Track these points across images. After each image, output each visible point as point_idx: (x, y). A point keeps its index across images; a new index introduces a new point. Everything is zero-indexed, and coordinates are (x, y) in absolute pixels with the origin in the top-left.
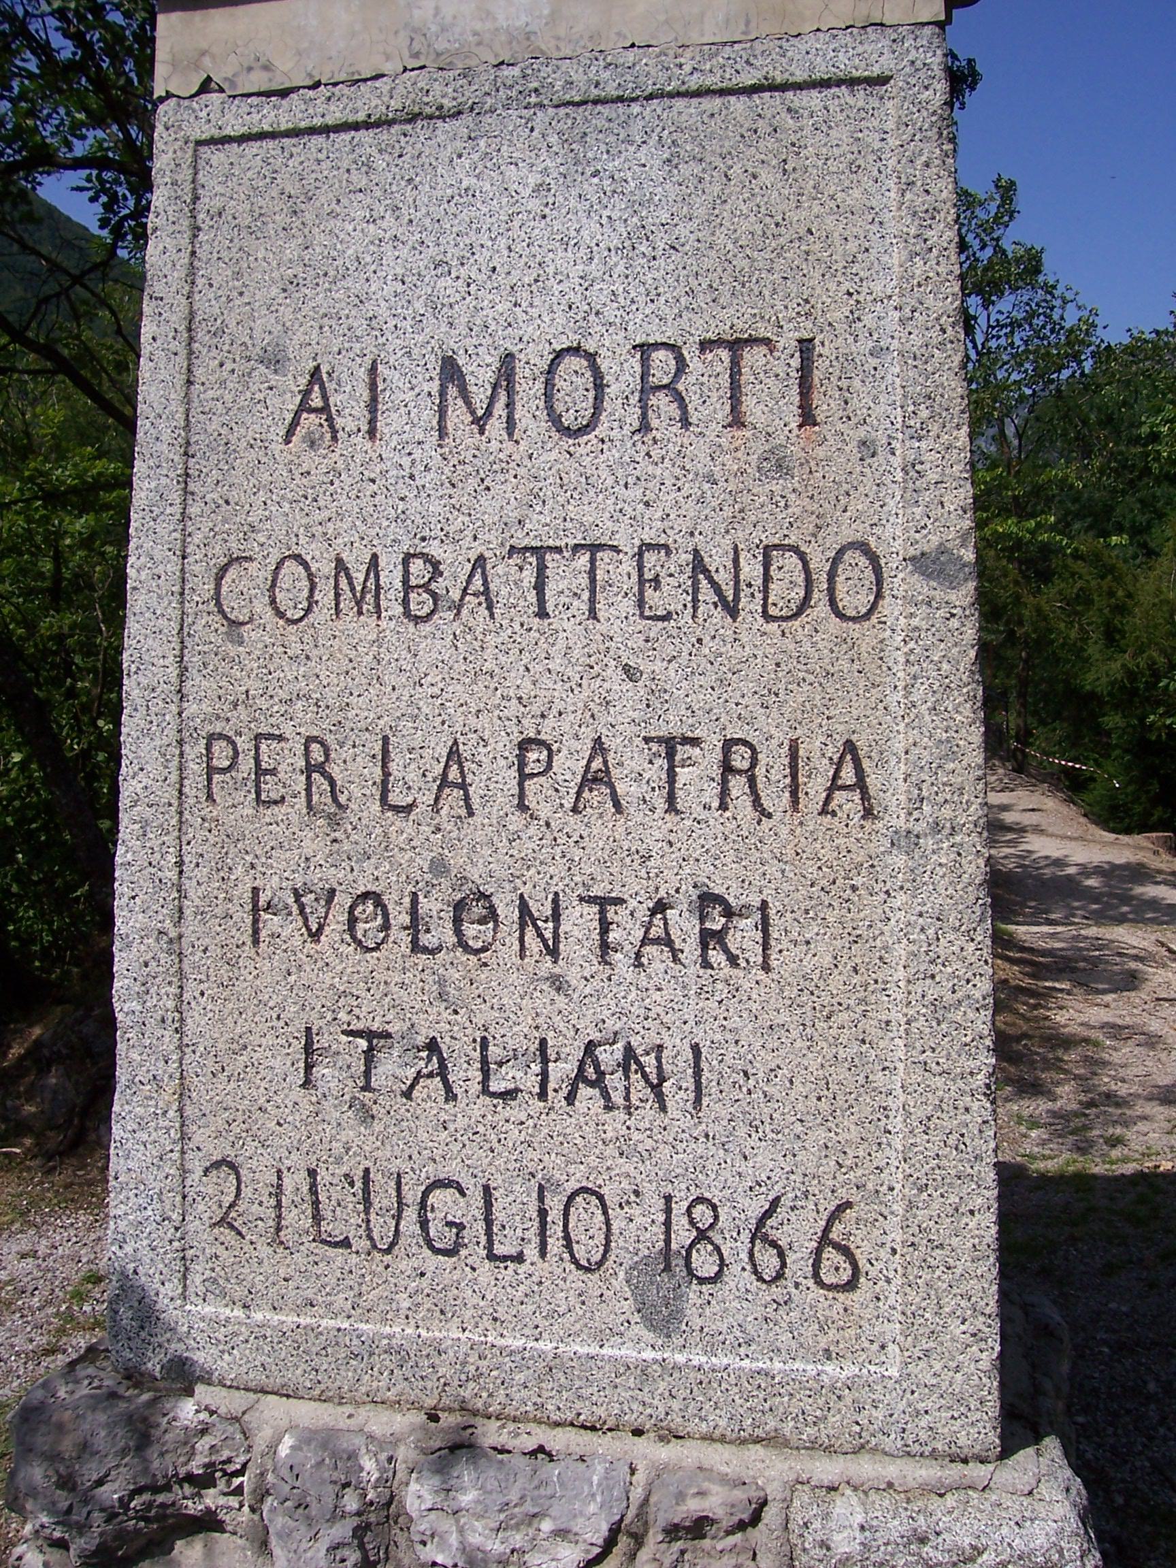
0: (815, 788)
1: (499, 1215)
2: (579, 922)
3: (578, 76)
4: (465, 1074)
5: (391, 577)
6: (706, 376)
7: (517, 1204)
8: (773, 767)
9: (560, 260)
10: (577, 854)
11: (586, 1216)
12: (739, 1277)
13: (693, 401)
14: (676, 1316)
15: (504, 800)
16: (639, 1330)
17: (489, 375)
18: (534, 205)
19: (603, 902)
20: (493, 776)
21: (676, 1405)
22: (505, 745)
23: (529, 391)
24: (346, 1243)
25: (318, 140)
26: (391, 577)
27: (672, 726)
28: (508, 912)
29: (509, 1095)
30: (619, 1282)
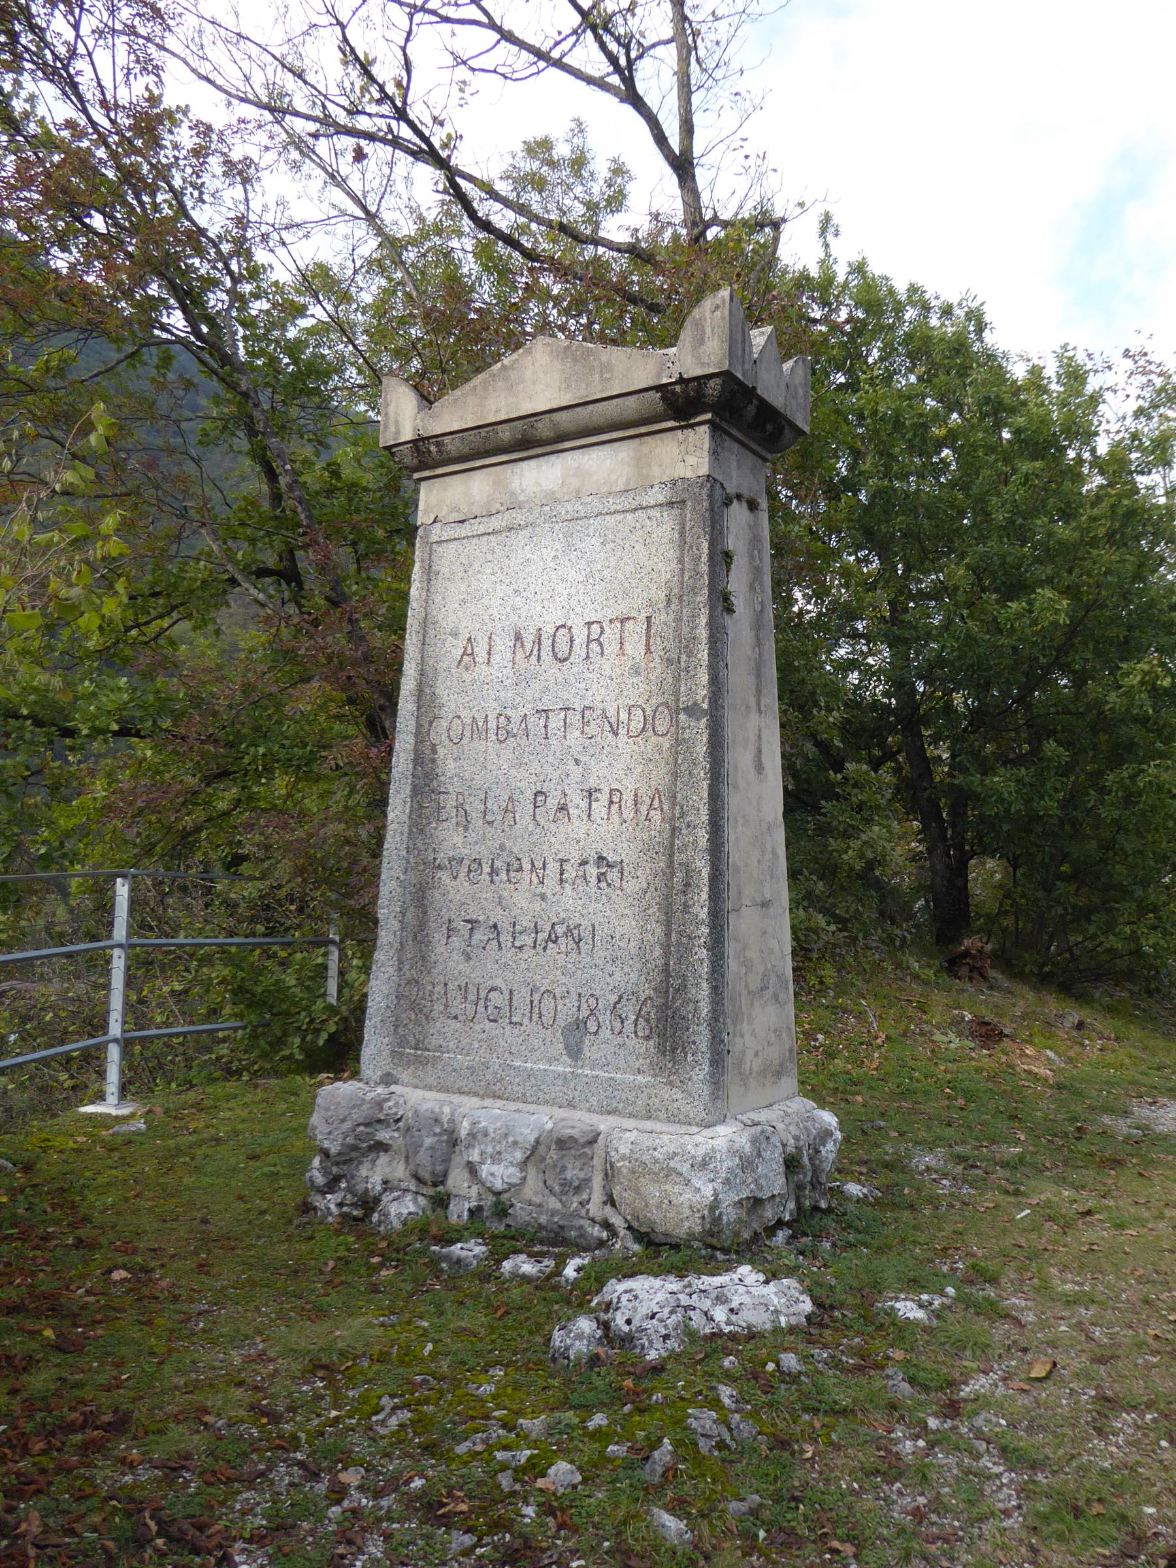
0: (644, 809)
1: (515, 1003)
2: (553, 868)
3: (570, 509)
4: (505, 938)
5: (492, 725)
6: (611, 634)
7: (521, 999)
8: (628, 798)
9: (560, 588)
10: (553, 840)
11: (548, 1003)
12: (605, 1033)
13: (606, 646)
14: (580, 1051)
15: (528, 818)
16: (565, 1058)
17: (531, 638)
18: (552, 565)
19: (562, 861)
20: (525, 807)
21: (577, 1094)
22: (529, 795)
23: (546, 643)
24: (456, 1017)
25: (475, 540)
26: (492, 725)
27: (592, 782)
28: (527, 866)
29: (521, 948)
30: (559, 1035)
